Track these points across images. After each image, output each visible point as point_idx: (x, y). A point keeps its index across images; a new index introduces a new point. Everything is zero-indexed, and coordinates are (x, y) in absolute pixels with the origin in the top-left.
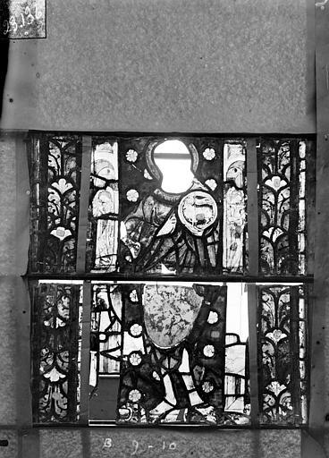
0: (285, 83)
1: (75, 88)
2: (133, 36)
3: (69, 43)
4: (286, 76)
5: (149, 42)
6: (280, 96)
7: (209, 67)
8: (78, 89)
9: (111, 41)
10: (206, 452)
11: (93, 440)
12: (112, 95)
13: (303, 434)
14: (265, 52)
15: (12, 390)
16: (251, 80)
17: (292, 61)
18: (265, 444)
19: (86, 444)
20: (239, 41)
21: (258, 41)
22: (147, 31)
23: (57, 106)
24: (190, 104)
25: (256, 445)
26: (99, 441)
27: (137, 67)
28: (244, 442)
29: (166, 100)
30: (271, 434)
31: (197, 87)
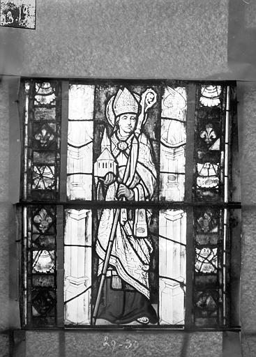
0: (203, 43)
1: (46, 44)
2: (90, 8)
3: (43, 11)
4: (205, 38)
5: (103, 13)
6: (200, 52)
7: (147, 32)
8: (48, 44)
9: (74, 12)
10: (151, 349)
11: (67, 338)
12: (74, 49)
13: (225, 337)
14: (188, 20)
15: (5, 289)
16: (178, 41)
17: (210, 27)
18: (195, 342)
19: (62, 340)
20: (170, 12)
21: (184, 11)
22: (100, 5)
23: (33, 57)
24: (132, 59)
25: (185, 343)
26: (71, 340)
27: (93, 30)
28: (178, 340)
29: (114, 55)
30: (201, 336)
31: (138, 47)
